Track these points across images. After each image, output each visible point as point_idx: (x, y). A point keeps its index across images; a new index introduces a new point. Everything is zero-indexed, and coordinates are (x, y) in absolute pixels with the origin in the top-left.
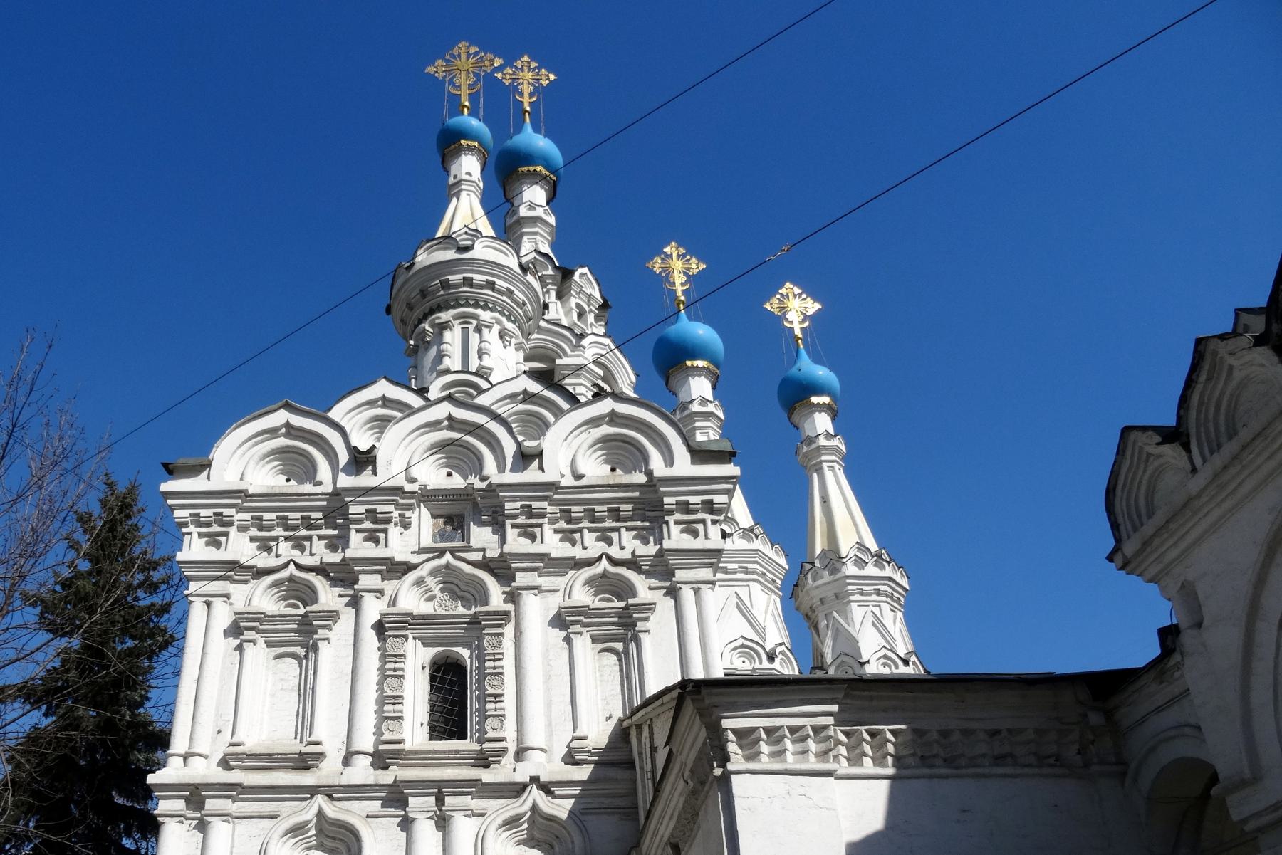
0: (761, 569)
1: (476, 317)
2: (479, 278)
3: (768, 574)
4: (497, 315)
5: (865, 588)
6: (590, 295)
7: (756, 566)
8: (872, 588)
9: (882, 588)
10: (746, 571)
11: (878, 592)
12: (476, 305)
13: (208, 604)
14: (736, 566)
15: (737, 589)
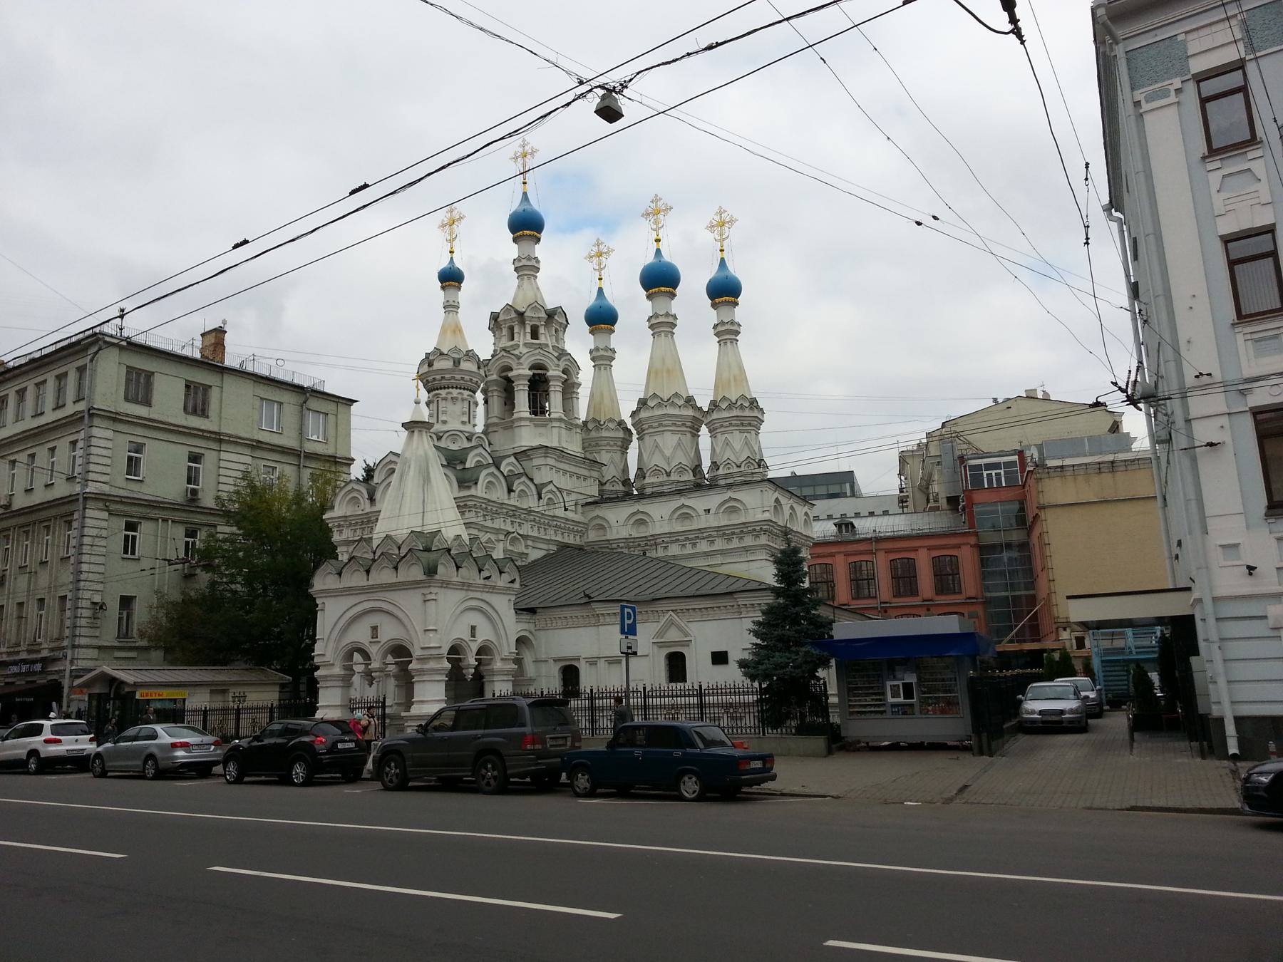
0: (670, 422)
1: (440, 394)
2: (438, 377)
3: (677, 423)
4: (450, 390)
5: (724, 424)
6: (539, 317)
7: (667, 422)
8: (727, 423)
9: (733, 422)
10: (661, 425)
11: (731, 424)
12: (441, 388)
13: (343, 554)
14: (657, 424)
15: (655, 438)
